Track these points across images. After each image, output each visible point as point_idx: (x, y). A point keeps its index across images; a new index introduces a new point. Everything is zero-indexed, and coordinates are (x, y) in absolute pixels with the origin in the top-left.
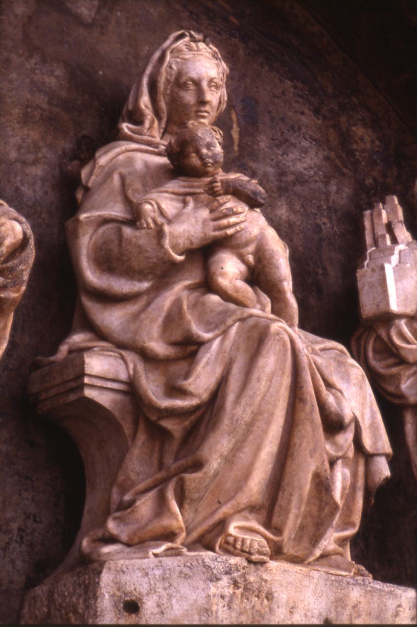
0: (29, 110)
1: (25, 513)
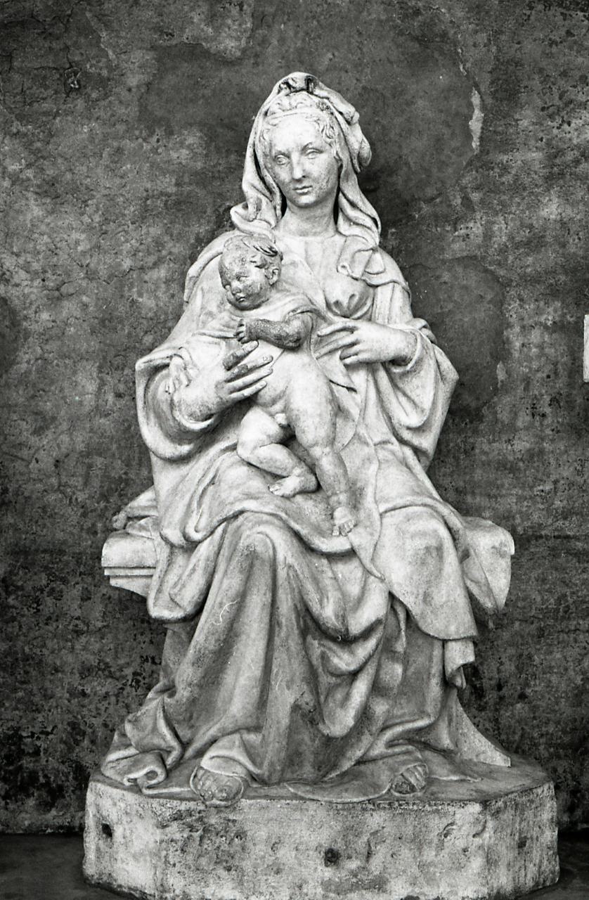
0: (149, 202)
1: (142, 657)
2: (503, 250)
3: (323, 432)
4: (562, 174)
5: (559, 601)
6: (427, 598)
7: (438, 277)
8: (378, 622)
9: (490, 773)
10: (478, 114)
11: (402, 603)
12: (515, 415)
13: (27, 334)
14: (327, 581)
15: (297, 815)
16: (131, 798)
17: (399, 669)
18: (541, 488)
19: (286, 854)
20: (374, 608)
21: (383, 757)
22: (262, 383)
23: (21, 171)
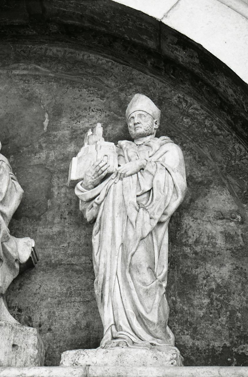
2: (53, 162)
5: (67, 290)
7: (27, 171)
12: (54, 218)
18: (63, 245)
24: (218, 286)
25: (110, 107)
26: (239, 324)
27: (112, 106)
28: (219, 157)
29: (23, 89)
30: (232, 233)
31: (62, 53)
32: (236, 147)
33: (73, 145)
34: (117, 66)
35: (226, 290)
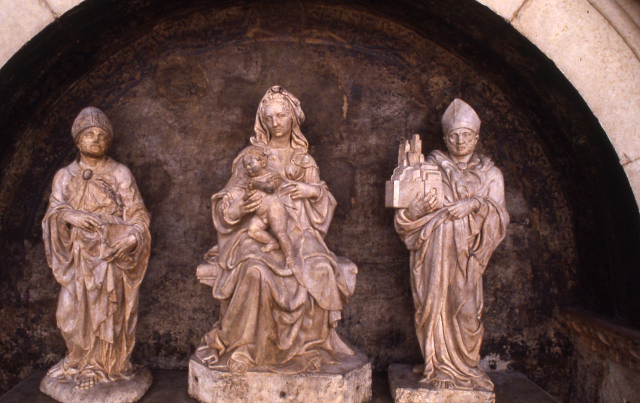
2: (355, 155)
3: (281, 227)
4: (377, 128)
5: (373, 288)
6: (322, 294)
7: (330, 165)
8: (303, 305)
9: (346, 359)
10: (346, 104)
11: (312, 296)
13: (174, 184)
14: (282, 287)
15: (269, 378)
16: (204, 369)
17: (311, 322)
19: (264, 393)
20: (302, 298)
21: (304, 355)
22: (258, 207)
23: (173, 123)
24: (503, 286)
25: (411, 92)
26: (516, 318)
27: (413, 90)
28: (517, 157)
29: (318, 63)
30: (520, 236)
31: (359, 19)
32: (534, 146)
33: (375, 137)
34: (419, 40)
35: (508, 290)
